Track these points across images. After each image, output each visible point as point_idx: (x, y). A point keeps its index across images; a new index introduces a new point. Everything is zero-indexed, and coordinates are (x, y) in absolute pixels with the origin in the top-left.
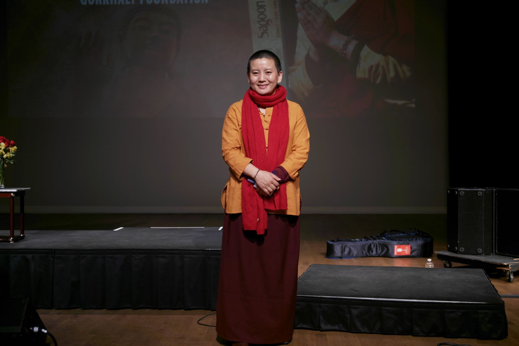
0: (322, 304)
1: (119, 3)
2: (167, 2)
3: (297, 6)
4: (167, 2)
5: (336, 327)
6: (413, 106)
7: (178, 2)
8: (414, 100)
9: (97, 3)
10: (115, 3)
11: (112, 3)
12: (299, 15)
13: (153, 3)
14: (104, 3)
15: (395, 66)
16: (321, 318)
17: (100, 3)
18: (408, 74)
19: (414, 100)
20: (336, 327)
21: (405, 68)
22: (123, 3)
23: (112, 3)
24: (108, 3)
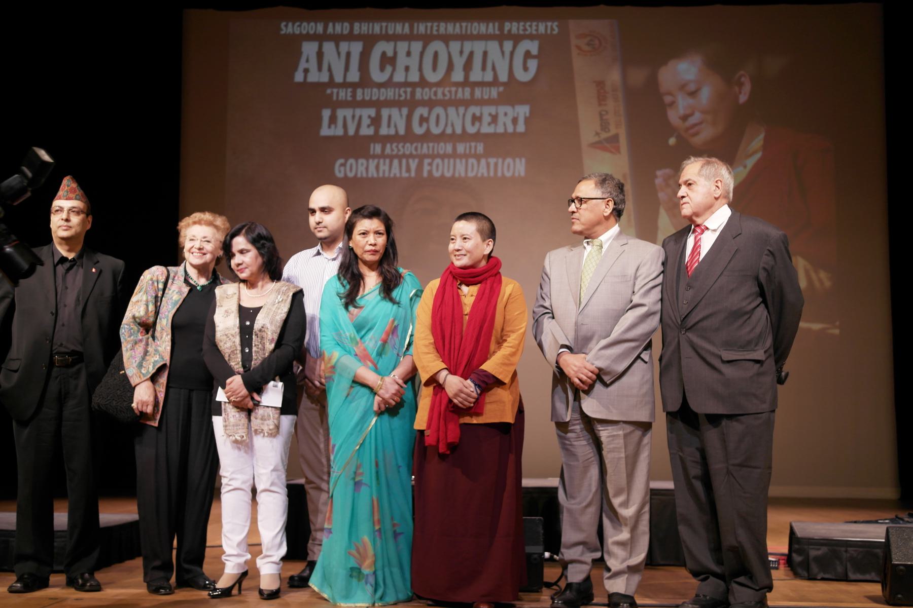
0: (849, 549)
1: (392, 175)
2: (463, 175)
3: (658, 181)
4: (463, 175)
5: (868, 577)
6: (837, 332)
7: (479, 175)
8: (838, 323)
9: (359, 175)
10: (387, 175)
11: (381, 175)
12: (661, 195)
13: (443, 176)
14: (370, 175)
15: (807, 272)
16: (849, 565)
17: (364, 175)
18: (828, 284)
19: (838, 323)
20: (868, 577)
21: (823, 275)
22: (398, 175)
23: (381, 175)
24: (375, 175)
